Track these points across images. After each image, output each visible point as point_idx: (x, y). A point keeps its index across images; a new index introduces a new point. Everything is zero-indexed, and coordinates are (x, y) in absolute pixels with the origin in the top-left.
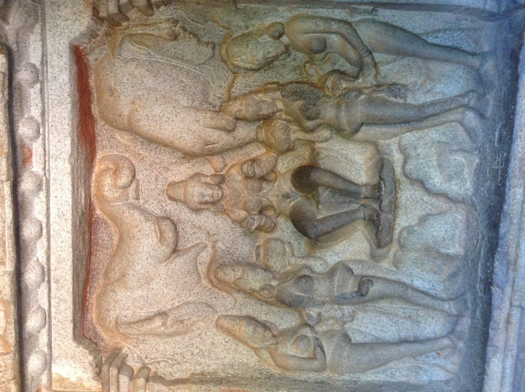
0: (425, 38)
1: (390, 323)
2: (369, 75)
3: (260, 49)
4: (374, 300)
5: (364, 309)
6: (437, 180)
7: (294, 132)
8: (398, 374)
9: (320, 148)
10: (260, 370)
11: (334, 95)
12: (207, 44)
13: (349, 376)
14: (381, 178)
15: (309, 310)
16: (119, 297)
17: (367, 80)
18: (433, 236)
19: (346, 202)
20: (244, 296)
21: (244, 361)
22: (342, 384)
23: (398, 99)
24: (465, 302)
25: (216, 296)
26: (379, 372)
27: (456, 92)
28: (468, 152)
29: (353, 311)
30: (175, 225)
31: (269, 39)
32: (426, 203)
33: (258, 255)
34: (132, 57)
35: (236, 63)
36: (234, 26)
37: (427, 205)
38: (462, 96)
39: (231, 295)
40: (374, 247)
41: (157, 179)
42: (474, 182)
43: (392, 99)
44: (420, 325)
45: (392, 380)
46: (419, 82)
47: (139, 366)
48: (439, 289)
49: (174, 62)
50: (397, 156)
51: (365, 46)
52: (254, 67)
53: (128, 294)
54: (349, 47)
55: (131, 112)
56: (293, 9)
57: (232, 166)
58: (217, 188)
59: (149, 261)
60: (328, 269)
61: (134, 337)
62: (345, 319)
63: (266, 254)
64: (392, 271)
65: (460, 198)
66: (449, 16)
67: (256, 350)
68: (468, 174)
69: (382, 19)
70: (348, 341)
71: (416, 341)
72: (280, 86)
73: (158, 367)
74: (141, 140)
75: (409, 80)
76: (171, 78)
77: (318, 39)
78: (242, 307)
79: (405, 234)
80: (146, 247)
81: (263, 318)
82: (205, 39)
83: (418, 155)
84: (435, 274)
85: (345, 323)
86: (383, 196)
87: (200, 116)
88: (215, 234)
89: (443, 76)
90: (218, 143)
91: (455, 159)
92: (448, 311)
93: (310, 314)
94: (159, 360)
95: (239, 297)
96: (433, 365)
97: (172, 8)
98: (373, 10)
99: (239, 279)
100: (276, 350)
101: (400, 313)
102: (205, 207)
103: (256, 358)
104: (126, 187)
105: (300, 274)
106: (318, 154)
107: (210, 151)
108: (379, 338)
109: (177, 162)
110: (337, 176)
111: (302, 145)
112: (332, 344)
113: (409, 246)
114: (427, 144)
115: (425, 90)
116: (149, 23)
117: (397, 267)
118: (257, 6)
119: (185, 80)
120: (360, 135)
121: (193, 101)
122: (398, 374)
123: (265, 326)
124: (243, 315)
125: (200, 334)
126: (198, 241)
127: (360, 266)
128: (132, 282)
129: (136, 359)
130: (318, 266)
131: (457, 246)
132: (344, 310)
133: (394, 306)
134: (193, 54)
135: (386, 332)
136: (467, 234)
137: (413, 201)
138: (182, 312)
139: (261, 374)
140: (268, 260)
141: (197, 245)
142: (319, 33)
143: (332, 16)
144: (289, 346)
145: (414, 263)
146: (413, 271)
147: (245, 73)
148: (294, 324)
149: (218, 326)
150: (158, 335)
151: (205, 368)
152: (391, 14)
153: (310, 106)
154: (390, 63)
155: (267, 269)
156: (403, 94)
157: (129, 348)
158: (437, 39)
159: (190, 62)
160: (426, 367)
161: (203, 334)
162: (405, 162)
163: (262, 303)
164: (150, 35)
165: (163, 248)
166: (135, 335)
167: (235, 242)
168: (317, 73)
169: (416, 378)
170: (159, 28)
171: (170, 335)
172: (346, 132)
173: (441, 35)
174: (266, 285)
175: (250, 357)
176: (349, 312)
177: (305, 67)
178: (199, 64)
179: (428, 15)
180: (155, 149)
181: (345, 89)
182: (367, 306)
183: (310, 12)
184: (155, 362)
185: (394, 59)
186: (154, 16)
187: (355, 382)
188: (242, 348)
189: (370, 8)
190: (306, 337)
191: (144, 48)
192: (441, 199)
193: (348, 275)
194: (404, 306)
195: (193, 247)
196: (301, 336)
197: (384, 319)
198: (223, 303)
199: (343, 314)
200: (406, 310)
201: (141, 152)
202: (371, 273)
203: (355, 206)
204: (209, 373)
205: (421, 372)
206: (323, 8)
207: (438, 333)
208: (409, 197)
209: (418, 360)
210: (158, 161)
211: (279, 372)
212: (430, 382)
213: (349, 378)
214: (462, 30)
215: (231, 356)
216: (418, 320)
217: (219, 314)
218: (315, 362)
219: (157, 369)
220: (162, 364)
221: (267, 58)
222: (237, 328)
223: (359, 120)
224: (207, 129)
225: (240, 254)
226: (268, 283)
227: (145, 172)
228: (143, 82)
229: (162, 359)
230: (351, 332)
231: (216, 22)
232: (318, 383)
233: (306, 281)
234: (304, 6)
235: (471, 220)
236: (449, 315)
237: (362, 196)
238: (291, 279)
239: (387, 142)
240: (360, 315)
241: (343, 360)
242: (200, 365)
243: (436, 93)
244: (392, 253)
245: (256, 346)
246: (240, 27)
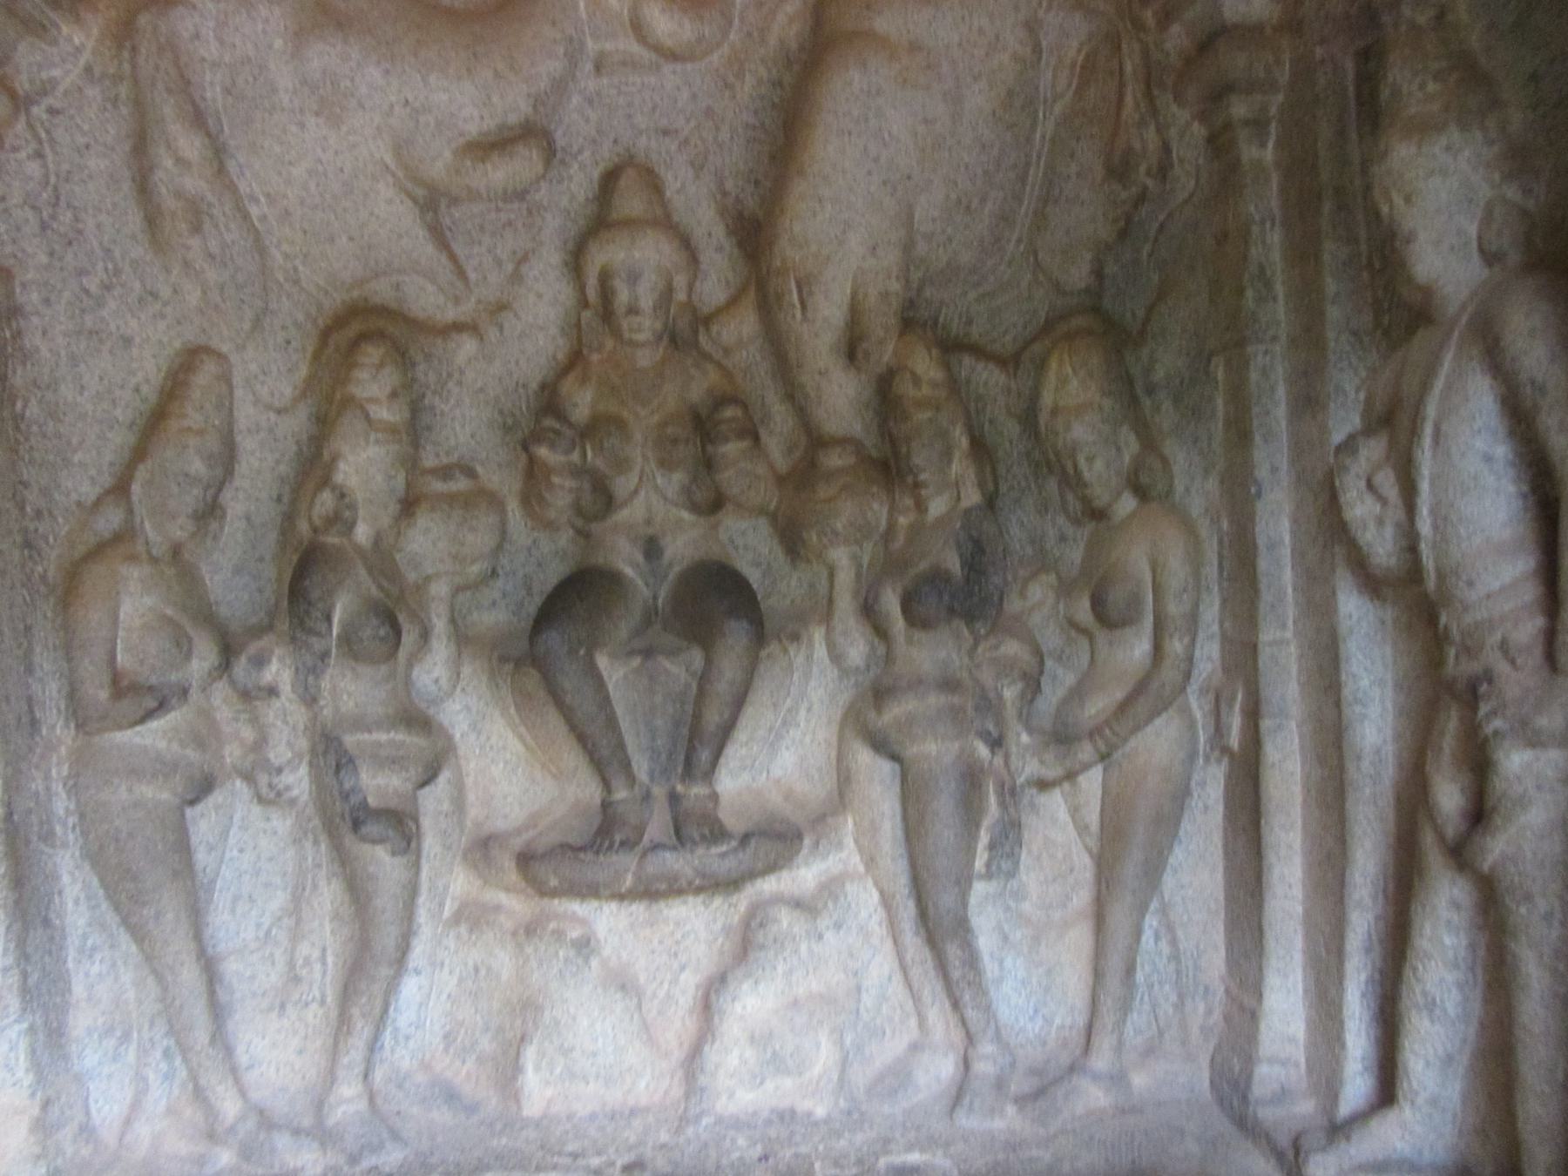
0: (1154, 905)
1: (267, 921)
2: (1042, 762)
4: (342, 859)
5: (305, 833)
6: (753, 1003)
7: (855, 558)
8: (95, 969)
9: (811, 645)
10: (50, 513)
11: (978, 666)
13: (67, 810)
14: (745, 839)
15: (281, 659)
16: (263, 11)
17: (1027, 758)
18: (574, 1019)
19: (653, 739)
20: (305, 437)
21: (75, 451)
22: (37, 794)
23: (986, 856)
24: (377, 1148)
25: (294, 344)
26: (98, 906)
27: (1004, 1013)
28: (841, 1079)
29: (293, 802)
30: (521, 195)
31: (1127, 459)
32: (675, 981)
33: (445, 473)
34: (1044, 43)
35: (1054, 364)
37: (666, 986)
38: (998, 1037)
39: (303, 395)
40: (518, 843)
41: (666, 133)
42: (755, 1113)
43: (984, 838)
44: (274, 1015)
45: (71, 954)
46: (1026, 907)
47: (17, 85)
48: (400, 1055)
49: (1036, 175)
50: (810, 876)
51: (1125, 740)
52: (1043, 418)
53: (278, 43)
54: (1119, 695)
55: (881, 42)
57: (727, 374)
58: (658, 325)
59: (397, 108)
60: (423, 705)
61: (126, 66)
62: (263, 779)
63: (451, 499)
64: (441, 905)
65: (702, 1080)
66: (1215, 962)
67: (120, 489)
68: (778, 1092)
69: (1196, 777)
70: (189, 797)
71: (218, 1012)
73: (23, 155)
74: (788, 79)
75: (1031, 877)
77: (1135, 601)
78: (262, 434)
79: (575, 933)
80: (445, 97)
81: (236, 504)
82: (1111, 269)
83: (820, 937)
84: (446, 1037)
85: (249, 778)
86: (692, 852)
87: (891, 258)
88: (501, 328)
89: (1049, 972)
90: (805, 318)
91: (818, 1045)
92: (332, 1099)
93: (269, 661)
94: (50, 157)
95: (297, 423)
96: (140, 1079)
97: (1201, 161)
98: (1225, 750)
99: (367, 416)
100: (133, 558)
101: (304, 949)
102: (592, 294)
103: (89, 492)
104: (638, 28)
105: (401, 618)
106: (795, 637)
107: (779, 297)
108: (210, 890)
109: (725, 194)
110: (739, 702)
111: (812, 586)
112: (175, 746)
113: (536, 950)
114: (851, 955)
115: (1006, 927)
116: (1156, 92)
117: (457, 918)
119: (989, 206)
120: (863, 757)
121: (929, 237)
122: (95, 969)
123: (209, 512)
124: (239, 438)
125: (154, 295)
126: (472, 276)
127: (446, 806)
128: (324, 55)
129: (44, 75)
130: (433, 670)
131: (549, 1092)
132: (294, 769)
133: (328, 928)
134: (1068, 232)
135: (233, 911)
136: (593, 1117)
137: (677, 943)
138: (228, 230)
139: (38, 514)
140: (433, 509)
141: (461, 273)
142: (1155, 600)
143: (1201, 635)
144: (149, 601)
145: (477, 970)
146: (446, 969)
147: (1019, 395)
148: (224, 611)
149: (190, 358)
150: (141, 145)
151: (35, 320)
152: (1210, 802)
153: (946, 597)
154: (1073, 817)
155: (409, 505)
156: (999, 867)
157: (78, 50)
158: (1152, 941)
159: (1040, 220)
160: (131, 1056)
161: (158, 306)
162: (798, 904)
163: (286, 499)
165: (447, 154)
166: (134, 67)
167: (481, 396)
168: (1032, 609)
169: (89, 1031)
170: (1142, 124)
171: (144, 188)
172: (872, 715)
173: (1165, 947)
174: (352, 507)
175: (93, 472)
176: (288, 788)
179: (1213, 906)
180: (763, 124)
181: (1000, 697)
182: (316, 842)
183: (1211, 571)
184: (40, 142)
185: (1087, 827)
187: (48, 837)
188: (120, 440)
189: (1234, 740)
190: (188, 656)
191: (1075, 82)
192: (692, 1025)
193: (414, 773)
194: (330, 960)
195: (453, 258)
196: (190, 640)
197: (279, 900)
198: (274, 368)
199: (279, 771)
200: (318, 967)
201: (749, 80)
202: (430, 844)
203: (641, 766)
204: (18, 335)
205: (111, 1043)
207: (250, 1078)
208: (688, 927)
209: (152, 1024)
210: (724, 135)
211: (50, 574)
212: (79, 1079)
213: (61, 812)
214: (1180, 1006)
215: (90, 407)
216: (289, 1007)
217: (234, 358)
218: (104, 695)
219: (15, 149)
220: (33, 168)
221: (1073, 456)
222: (194, 419)
223: (911, 751)
224: (849, 285)
225: (442, 414)
226: (361, 513)
227: (685, 94)
228: (975, 79)
229: (51, 166)
230: (220, 799)
232: (31, 711)
233: (382, 639)
234: (1225, 552)
235: (637, 1123)
236: (319, 1105)
237: (679, 788)
238: (380, 587)
239: (849, 842)
240: (282, 823)
241: (124, 787)
242: (47, 301)
243: (1001, 962)
244: (503, 898)
245: (136, 488)
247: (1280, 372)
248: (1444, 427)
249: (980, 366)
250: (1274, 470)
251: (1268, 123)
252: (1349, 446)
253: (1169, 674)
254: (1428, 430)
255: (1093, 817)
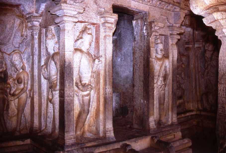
3: (18, 63)
12: (19, 46)
31: (21, 66)
36: (24, 55)
51: (20, 96)
54: (20, 91)
56: (30, 73)
69: (28, 100)
72: (6, 69)
76: (9, 33)
82: (20, 45)
116: (27, 29)
118: (31, 62)
119: (8, 37)
143: (28, 85)
164: (23, 29)
168: (10, 82)
170: (25, 32)
173: (24, 118)
177: (12, 78)
178: (13, 43)
181: (7, 91)
183: (30, 78)
185: (16, 106)
186: (28, 31)
189: (32, 96)
206: (31, 82)
221: (16, 65)
231: (25, 49)
246: (24, 57)
247: (37, 58)
248: (50, 65)
249: (6, 55)
250: (36, 68)
251: (37, 34)
252: (42, 66)
253: (25, 89)
254: (48, 65)
255: (17, 105)
